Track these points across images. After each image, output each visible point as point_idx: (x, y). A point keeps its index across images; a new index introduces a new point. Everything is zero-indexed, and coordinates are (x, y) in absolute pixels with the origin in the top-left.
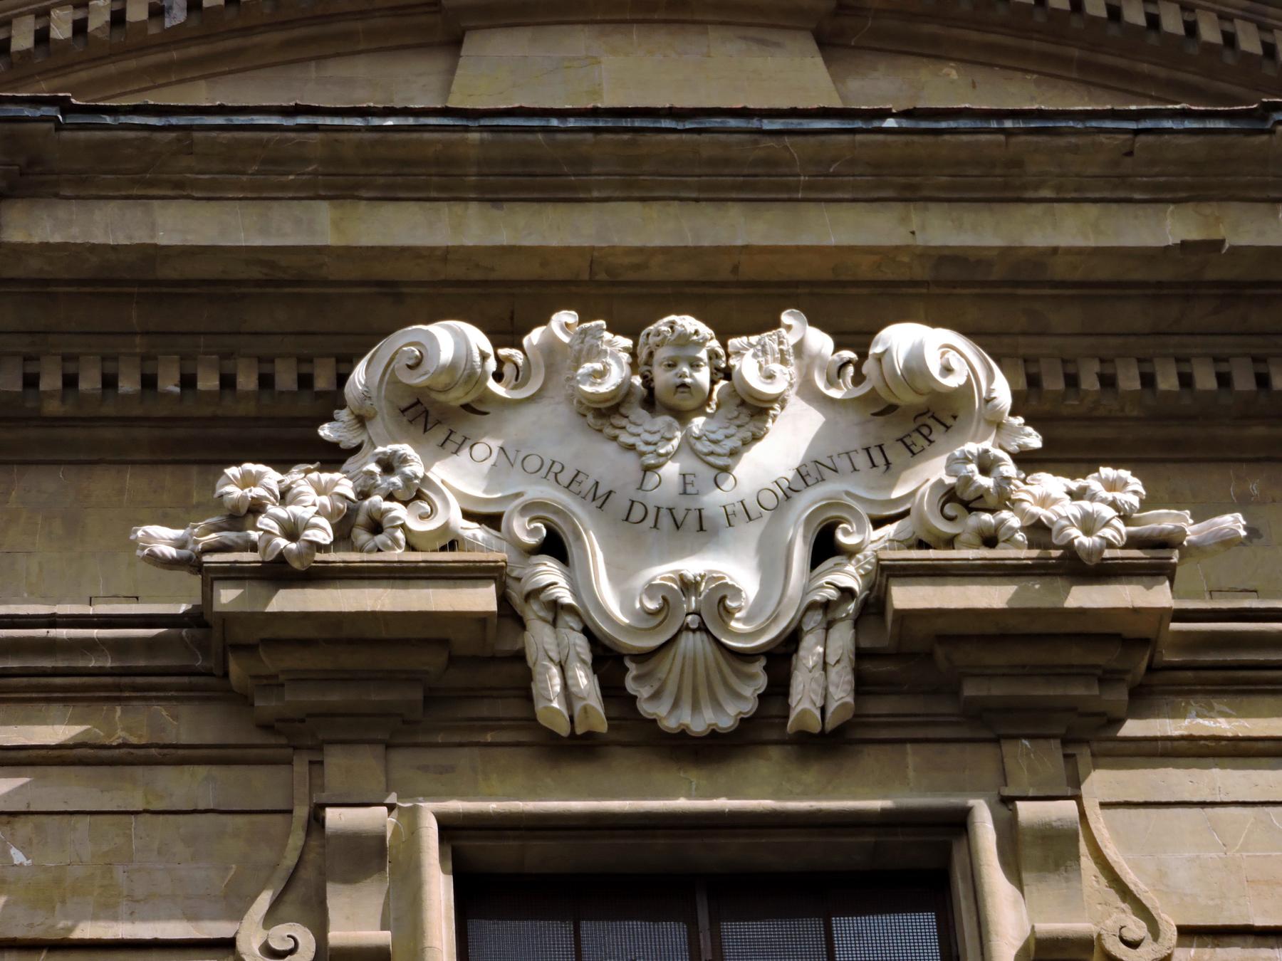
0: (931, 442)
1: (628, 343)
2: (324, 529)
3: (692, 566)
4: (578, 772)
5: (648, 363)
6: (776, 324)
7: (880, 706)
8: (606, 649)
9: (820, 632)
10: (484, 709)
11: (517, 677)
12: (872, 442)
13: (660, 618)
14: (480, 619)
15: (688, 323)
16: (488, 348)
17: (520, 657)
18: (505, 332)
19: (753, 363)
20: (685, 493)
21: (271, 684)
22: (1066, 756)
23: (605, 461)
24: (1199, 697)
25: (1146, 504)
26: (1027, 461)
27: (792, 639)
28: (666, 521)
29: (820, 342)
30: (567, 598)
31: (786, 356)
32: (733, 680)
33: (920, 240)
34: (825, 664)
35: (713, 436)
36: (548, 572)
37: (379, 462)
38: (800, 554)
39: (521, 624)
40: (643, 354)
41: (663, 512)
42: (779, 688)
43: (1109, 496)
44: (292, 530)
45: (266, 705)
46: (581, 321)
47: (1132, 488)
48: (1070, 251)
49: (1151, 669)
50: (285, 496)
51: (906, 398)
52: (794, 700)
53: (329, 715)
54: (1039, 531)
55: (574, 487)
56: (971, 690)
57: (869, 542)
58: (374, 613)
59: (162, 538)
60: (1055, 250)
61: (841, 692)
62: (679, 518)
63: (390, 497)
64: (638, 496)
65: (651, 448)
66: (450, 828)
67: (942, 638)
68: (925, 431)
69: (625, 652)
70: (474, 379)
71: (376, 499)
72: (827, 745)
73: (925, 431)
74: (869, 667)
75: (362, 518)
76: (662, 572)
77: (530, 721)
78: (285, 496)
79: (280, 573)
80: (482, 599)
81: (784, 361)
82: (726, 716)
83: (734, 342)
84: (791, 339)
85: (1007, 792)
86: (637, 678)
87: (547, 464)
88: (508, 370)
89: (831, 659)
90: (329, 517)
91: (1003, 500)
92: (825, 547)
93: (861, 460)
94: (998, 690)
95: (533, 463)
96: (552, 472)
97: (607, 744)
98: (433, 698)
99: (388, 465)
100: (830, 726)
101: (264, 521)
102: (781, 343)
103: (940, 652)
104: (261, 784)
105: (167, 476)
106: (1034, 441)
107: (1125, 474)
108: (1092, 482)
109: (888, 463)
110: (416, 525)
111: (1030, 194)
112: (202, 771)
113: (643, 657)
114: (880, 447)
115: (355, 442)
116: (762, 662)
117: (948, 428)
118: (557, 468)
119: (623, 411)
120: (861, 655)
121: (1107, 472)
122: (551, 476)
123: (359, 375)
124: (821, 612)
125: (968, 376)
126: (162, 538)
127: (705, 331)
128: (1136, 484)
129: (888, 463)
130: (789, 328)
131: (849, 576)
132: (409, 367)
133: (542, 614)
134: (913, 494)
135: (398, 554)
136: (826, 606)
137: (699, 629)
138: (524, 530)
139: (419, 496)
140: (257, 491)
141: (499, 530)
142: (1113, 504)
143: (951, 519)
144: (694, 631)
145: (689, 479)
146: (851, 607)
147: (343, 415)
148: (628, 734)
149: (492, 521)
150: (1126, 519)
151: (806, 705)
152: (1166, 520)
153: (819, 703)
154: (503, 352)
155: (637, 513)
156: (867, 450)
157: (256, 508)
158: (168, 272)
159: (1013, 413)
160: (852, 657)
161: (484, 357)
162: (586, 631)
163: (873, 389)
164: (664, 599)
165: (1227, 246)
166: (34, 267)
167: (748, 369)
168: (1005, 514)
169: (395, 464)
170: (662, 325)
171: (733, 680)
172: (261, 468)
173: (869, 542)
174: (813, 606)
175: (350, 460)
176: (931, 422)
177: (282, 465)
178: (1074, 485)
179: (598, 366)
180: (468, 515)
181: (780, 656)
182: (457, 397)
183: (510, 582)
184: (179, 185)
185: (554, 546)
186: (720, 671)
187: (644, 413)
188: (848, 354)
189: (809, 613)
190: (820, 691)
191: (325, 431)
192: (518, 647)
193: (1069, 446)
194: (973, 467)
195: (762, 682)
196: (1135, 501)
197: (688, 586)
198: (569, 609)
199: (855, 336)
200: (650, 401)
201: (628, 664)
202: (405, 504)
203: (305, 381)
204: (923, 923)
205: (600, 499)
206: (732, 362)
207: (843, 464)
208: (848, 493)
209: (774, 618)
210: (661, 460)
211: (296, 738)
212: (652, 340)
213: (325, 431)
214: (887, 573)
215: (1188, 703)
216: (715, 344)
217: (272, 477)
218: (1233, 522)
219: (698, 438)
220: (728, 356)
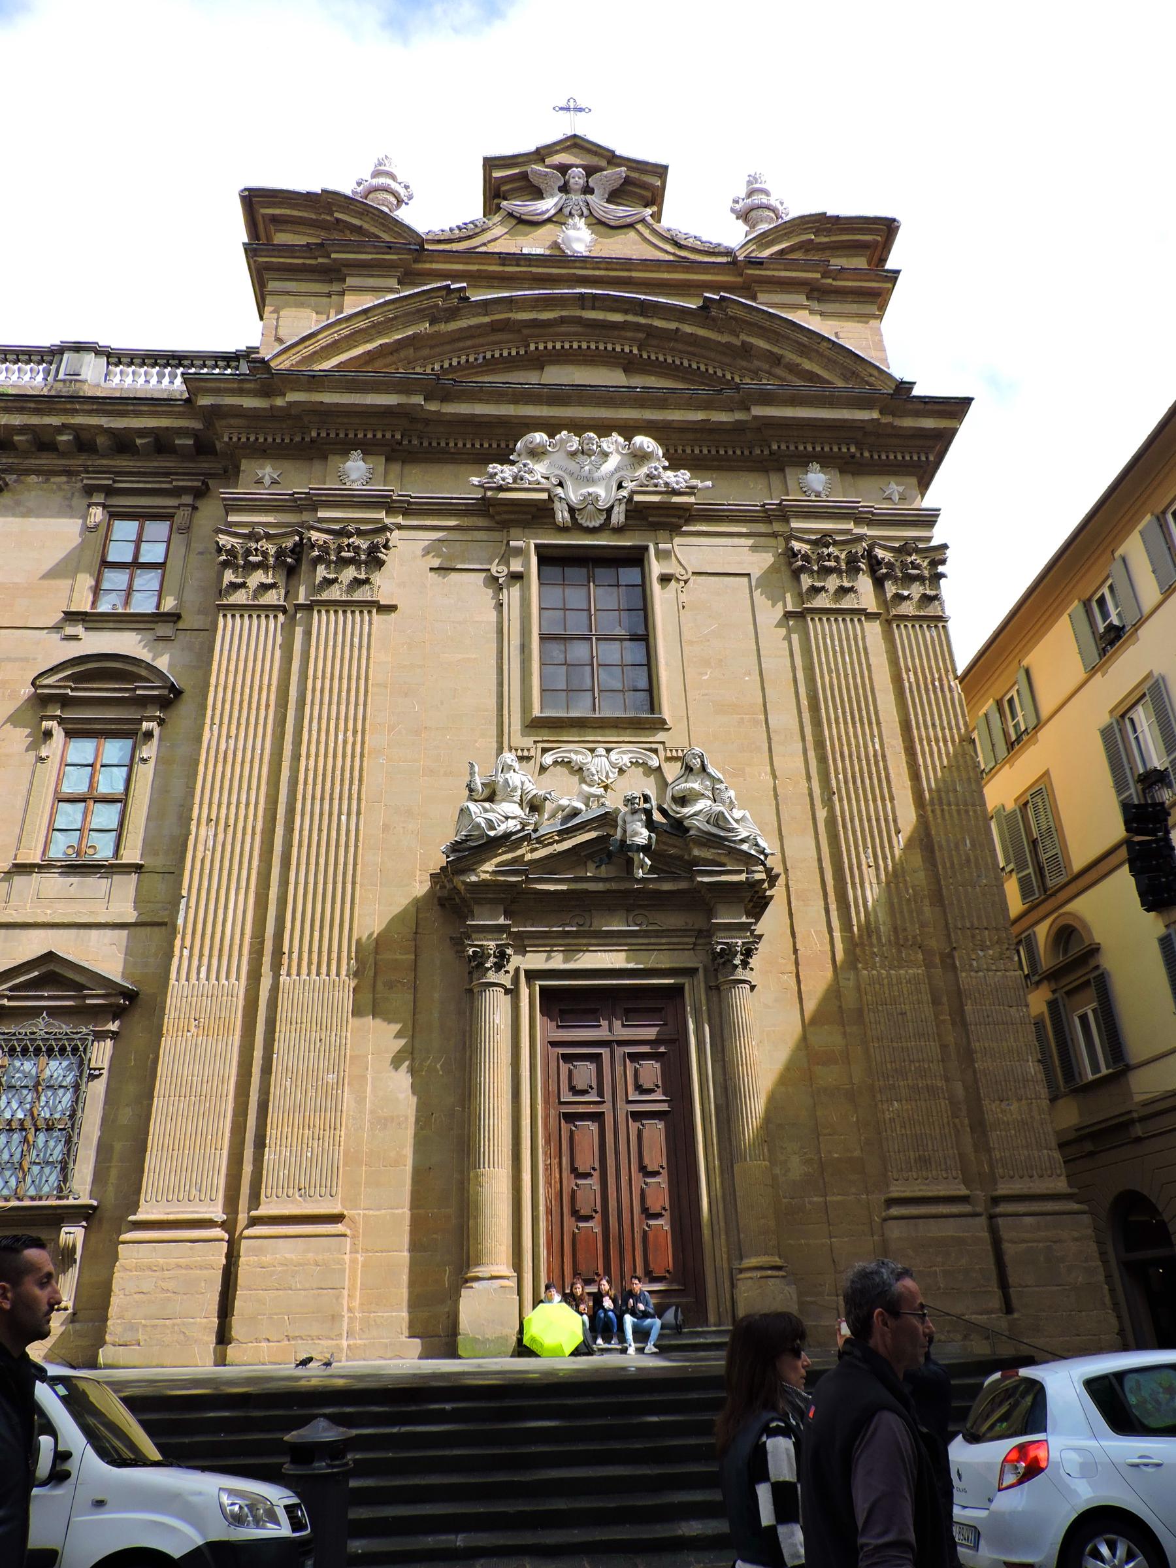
3: (591, 490)
4: (565, 535)
7: (629, 522)
11: (552, 513)
15: (592, 434)
18: (551, 435)
21: (499, 513)
23: (572, 465)
26: (665, 468)
27: (612, 507)
29: (621, 440)
31: (614, 442)
36: (559, 490)
38: (615, 487)
42: (609, 518)
44: (503, 479)
45: (497, 518)
50: (502, 472)
51: (639, 453)
53: (512, 521)
54: (667, 484)
57: (629, 485)
59: (475, 480)
61: (622, 519)
66: (536, 546)
70: (544, 446)
72: (619, 530)
76: (584, 491)
78: (502, 472)
79: (501, 489)
80: (544, 496)
82: (596, 523)
91: (659, 477)
92: (620, 486)
96: (561, 468)
98: (534, 517)
99: (525, 465)
104: (496, 535)
105: (477, 466)
106: (667, 464)
113: (579, 510)
120: (627, 511)
123: (519, 444)
126: (475, 480)
131: (625, 493)
135: (527, 485)
138: (555, 481)
148: (576, 527)
149: (547, 478)
152: (695, 482)
157: (496, 474)
158: (477, 420)
166: (448, 418)
167: (605, 446)
173: (629, 485)
177: (502, 464)
181: (609, 511)
182: (540, 450)
185: (561, 484)
193: (674, 466)
197: (590, 494)
199: (628, 438)
200: (583, 452)
203: (507, 446)
204: (637, 570)
205: (571, 474)
211: (504, 525)
214: (633, 492)
217: (499, 467)
218: (709, 483)
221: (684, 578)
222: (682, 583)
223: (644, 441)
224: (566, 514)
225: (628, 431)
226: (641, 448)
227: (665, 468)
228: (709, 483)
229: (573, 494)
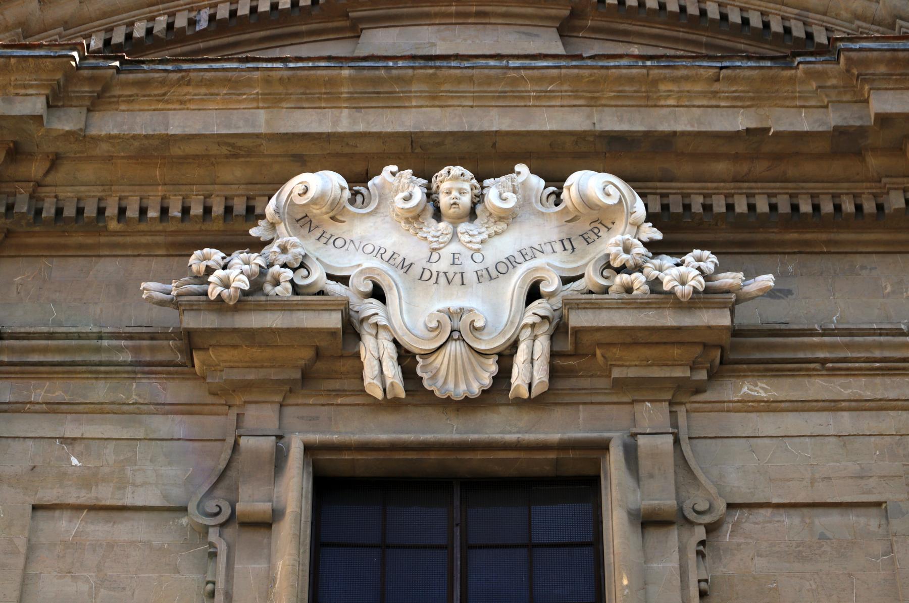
0: (599, 237)
1: (425, 182)
2: (244, 282)
3: (454, 304)
5: (437, 193)
6: (512, 171)
8: (407, 351)
9: (529, 342)
10: (336, 385)
12: (564, 236)
13: (436, 333)
14: (332, 333)
16: (345, 184)
17: (358, 356)
18: (358, 178)
19: (498, 193)
20: (454, 263)
22: (670, 412)
24: (750, 379)
25: (719, 269)
27: (514, 346)
28: (442, 280)
29: (538, 182)
30: (383, 321)
32: (478, 369)
33: (598, 128)
34: (532, 359)
35: (471, 233)
36: (373, 306)
37: (279, 246)
39: (358, 337)
40: (434, 186)
41: (441, 274)
43: (697, 264)
46: (400, 170)
47: (710, 260)
48: (683, 133)
49: (721, 363)
52: (513, 381)
54: (655, 285)
55: (391, 261)
56: (616, 373)
58: (271, 329)
60: (675, 133)
61: (541, 375)
62: (450, 279)
63: (285, 266)
64: (428, 266)
65: (436, 239)
66: (309, 449)
67: (600, 345)
68: (596, 231)
69: (416, 351)
71: (276, 268)
73: (596, 231)
74: (558, 362)
75: (269, 278)
77: (362, 392)
80: (333, 321)
81: (514, 192)
83: (486, 182)
84: (520, 179)
85: (634, 430)
86: (423, 366)
87: (377, 249)
88: (359, 198)
89: (535, 357)
90: (249, 277)
92: (534, 294)
93: (558, 247)
94: (632, 373)
95: (369, 248)
97: (407, 405)
100: (533, 396)
101: (211, 278)
102: (512, 181)
103: (598, 352)
106: (658, 235)
107: (707, 253)
108: (688, 258)
109: (573, 248)
110: (300, 282)
111: (662, 103)
112: (178, 418)
113: (427, 355)
114: (570, 239)
115: (268, 238)
116: (496, 358)
117: (609, 229)
118: (382, 251)
119: (420, 219)
120: (554, 355)
121: (697, 252)
122: (379, 255)
124: (529, 329)
125: (620, 199)
127: (469, 174)
128: (714, 258)
129: (573, 248)
130: (519, 173)
132: (300, 195)
133: (369, 331)
134: (586, 265)
136: (533, 326)
137: (458, 339)
139: (302, 265)
140: (210, 263)
141: (348, 285)
142: (699, 269)
143: (607, 278)
144: (456, 340)
145: (456, 256)
146: (546, 327)
147: (261, 223)
150: (707, 278)
151: (519, 382)
152: (729, 279)
153: (528, 381)
154: (355, 188)
155: (427, 275)
156: (562, 241)
159: (646, 221)
160: (548, 356)
161: (342, 189)
162: (395, 341)
163: (566, 207)
164: (438, 321)
165: (772, 130)
168: (636, 275)
169: (289, 247)
170: (444, 171)
171: (478, 369)
172: (214, 250)
174: (525, 326)
175: (266, 247)
176: (599, 226)
178: (679, 260)
179: (406, 194)
180: (330, 277)
183: (352, 313)
184: (182, 102)
185: (378, 293)
186: (471, 363)
187: (434, 221)
188: (552, 189)
189: (523, 331)
190: (528, 374)
191: (254, 232)
192: (356, 350)
194: (621, 248)
195: (494, 368)
196: (712, 267)
198: (385, 327)
200: (438, 215)
201: (418, 358)
202: (294, 270)
206: (485, 191)
207: (548, 248)
208: (548, 264)
209: (502, 333)
210: (442, 245)
212: (438, 179)
213: (254, 232)
215: (743, 383)
216: (474, 181)
217: (216, 255)
218: (767, 280)
219: (462, 233)
220: (483, 188)
221: (707, 519)
222: (700, 533)
223: (590, 184)
224: (393, 372)
225: (555, 160)
226: (588, 204)
227: (650, 245)
228: (767, 280)
229: (412, 315)
